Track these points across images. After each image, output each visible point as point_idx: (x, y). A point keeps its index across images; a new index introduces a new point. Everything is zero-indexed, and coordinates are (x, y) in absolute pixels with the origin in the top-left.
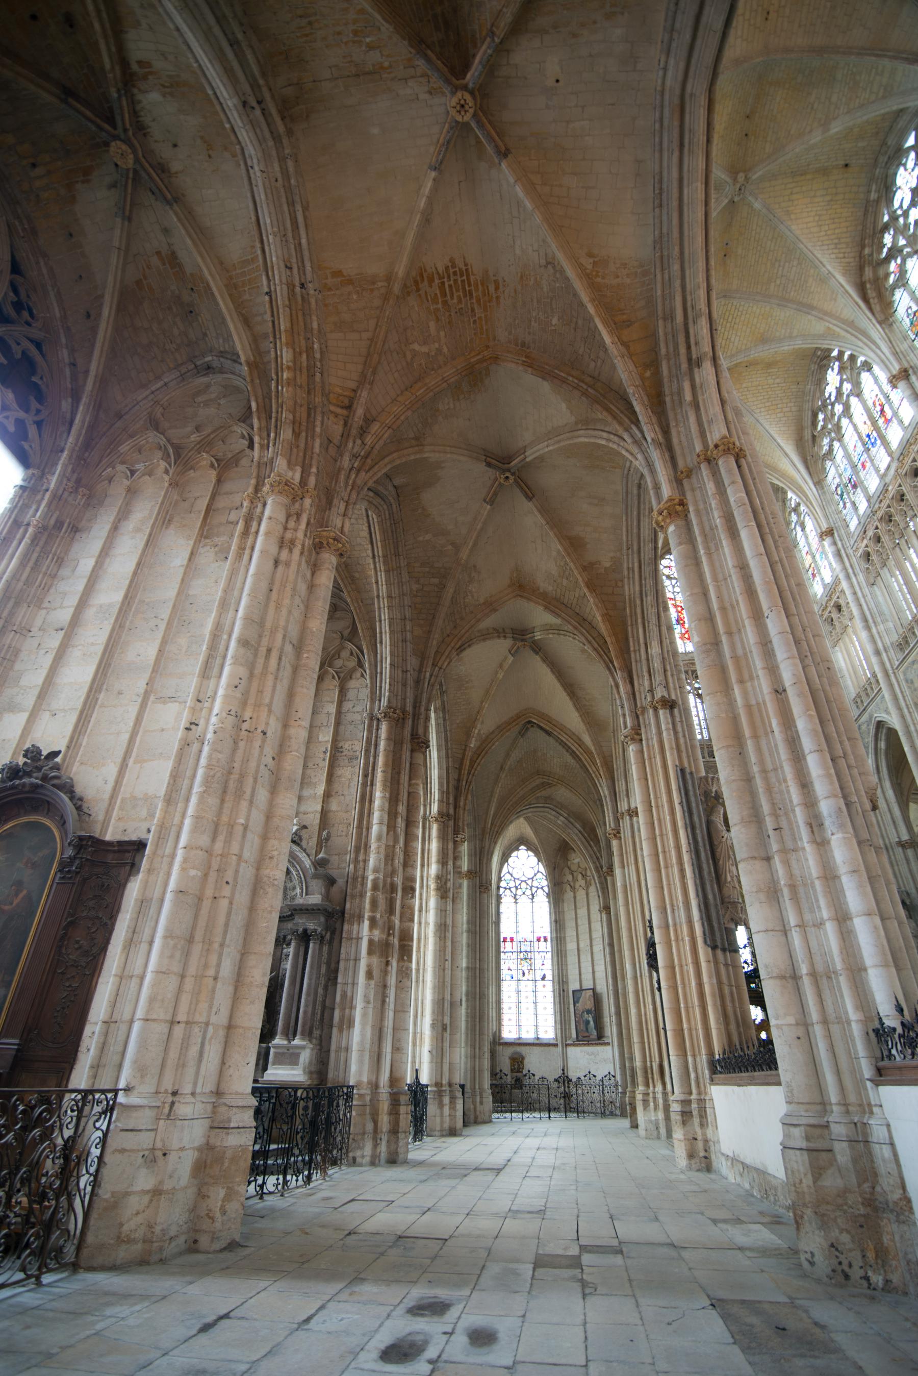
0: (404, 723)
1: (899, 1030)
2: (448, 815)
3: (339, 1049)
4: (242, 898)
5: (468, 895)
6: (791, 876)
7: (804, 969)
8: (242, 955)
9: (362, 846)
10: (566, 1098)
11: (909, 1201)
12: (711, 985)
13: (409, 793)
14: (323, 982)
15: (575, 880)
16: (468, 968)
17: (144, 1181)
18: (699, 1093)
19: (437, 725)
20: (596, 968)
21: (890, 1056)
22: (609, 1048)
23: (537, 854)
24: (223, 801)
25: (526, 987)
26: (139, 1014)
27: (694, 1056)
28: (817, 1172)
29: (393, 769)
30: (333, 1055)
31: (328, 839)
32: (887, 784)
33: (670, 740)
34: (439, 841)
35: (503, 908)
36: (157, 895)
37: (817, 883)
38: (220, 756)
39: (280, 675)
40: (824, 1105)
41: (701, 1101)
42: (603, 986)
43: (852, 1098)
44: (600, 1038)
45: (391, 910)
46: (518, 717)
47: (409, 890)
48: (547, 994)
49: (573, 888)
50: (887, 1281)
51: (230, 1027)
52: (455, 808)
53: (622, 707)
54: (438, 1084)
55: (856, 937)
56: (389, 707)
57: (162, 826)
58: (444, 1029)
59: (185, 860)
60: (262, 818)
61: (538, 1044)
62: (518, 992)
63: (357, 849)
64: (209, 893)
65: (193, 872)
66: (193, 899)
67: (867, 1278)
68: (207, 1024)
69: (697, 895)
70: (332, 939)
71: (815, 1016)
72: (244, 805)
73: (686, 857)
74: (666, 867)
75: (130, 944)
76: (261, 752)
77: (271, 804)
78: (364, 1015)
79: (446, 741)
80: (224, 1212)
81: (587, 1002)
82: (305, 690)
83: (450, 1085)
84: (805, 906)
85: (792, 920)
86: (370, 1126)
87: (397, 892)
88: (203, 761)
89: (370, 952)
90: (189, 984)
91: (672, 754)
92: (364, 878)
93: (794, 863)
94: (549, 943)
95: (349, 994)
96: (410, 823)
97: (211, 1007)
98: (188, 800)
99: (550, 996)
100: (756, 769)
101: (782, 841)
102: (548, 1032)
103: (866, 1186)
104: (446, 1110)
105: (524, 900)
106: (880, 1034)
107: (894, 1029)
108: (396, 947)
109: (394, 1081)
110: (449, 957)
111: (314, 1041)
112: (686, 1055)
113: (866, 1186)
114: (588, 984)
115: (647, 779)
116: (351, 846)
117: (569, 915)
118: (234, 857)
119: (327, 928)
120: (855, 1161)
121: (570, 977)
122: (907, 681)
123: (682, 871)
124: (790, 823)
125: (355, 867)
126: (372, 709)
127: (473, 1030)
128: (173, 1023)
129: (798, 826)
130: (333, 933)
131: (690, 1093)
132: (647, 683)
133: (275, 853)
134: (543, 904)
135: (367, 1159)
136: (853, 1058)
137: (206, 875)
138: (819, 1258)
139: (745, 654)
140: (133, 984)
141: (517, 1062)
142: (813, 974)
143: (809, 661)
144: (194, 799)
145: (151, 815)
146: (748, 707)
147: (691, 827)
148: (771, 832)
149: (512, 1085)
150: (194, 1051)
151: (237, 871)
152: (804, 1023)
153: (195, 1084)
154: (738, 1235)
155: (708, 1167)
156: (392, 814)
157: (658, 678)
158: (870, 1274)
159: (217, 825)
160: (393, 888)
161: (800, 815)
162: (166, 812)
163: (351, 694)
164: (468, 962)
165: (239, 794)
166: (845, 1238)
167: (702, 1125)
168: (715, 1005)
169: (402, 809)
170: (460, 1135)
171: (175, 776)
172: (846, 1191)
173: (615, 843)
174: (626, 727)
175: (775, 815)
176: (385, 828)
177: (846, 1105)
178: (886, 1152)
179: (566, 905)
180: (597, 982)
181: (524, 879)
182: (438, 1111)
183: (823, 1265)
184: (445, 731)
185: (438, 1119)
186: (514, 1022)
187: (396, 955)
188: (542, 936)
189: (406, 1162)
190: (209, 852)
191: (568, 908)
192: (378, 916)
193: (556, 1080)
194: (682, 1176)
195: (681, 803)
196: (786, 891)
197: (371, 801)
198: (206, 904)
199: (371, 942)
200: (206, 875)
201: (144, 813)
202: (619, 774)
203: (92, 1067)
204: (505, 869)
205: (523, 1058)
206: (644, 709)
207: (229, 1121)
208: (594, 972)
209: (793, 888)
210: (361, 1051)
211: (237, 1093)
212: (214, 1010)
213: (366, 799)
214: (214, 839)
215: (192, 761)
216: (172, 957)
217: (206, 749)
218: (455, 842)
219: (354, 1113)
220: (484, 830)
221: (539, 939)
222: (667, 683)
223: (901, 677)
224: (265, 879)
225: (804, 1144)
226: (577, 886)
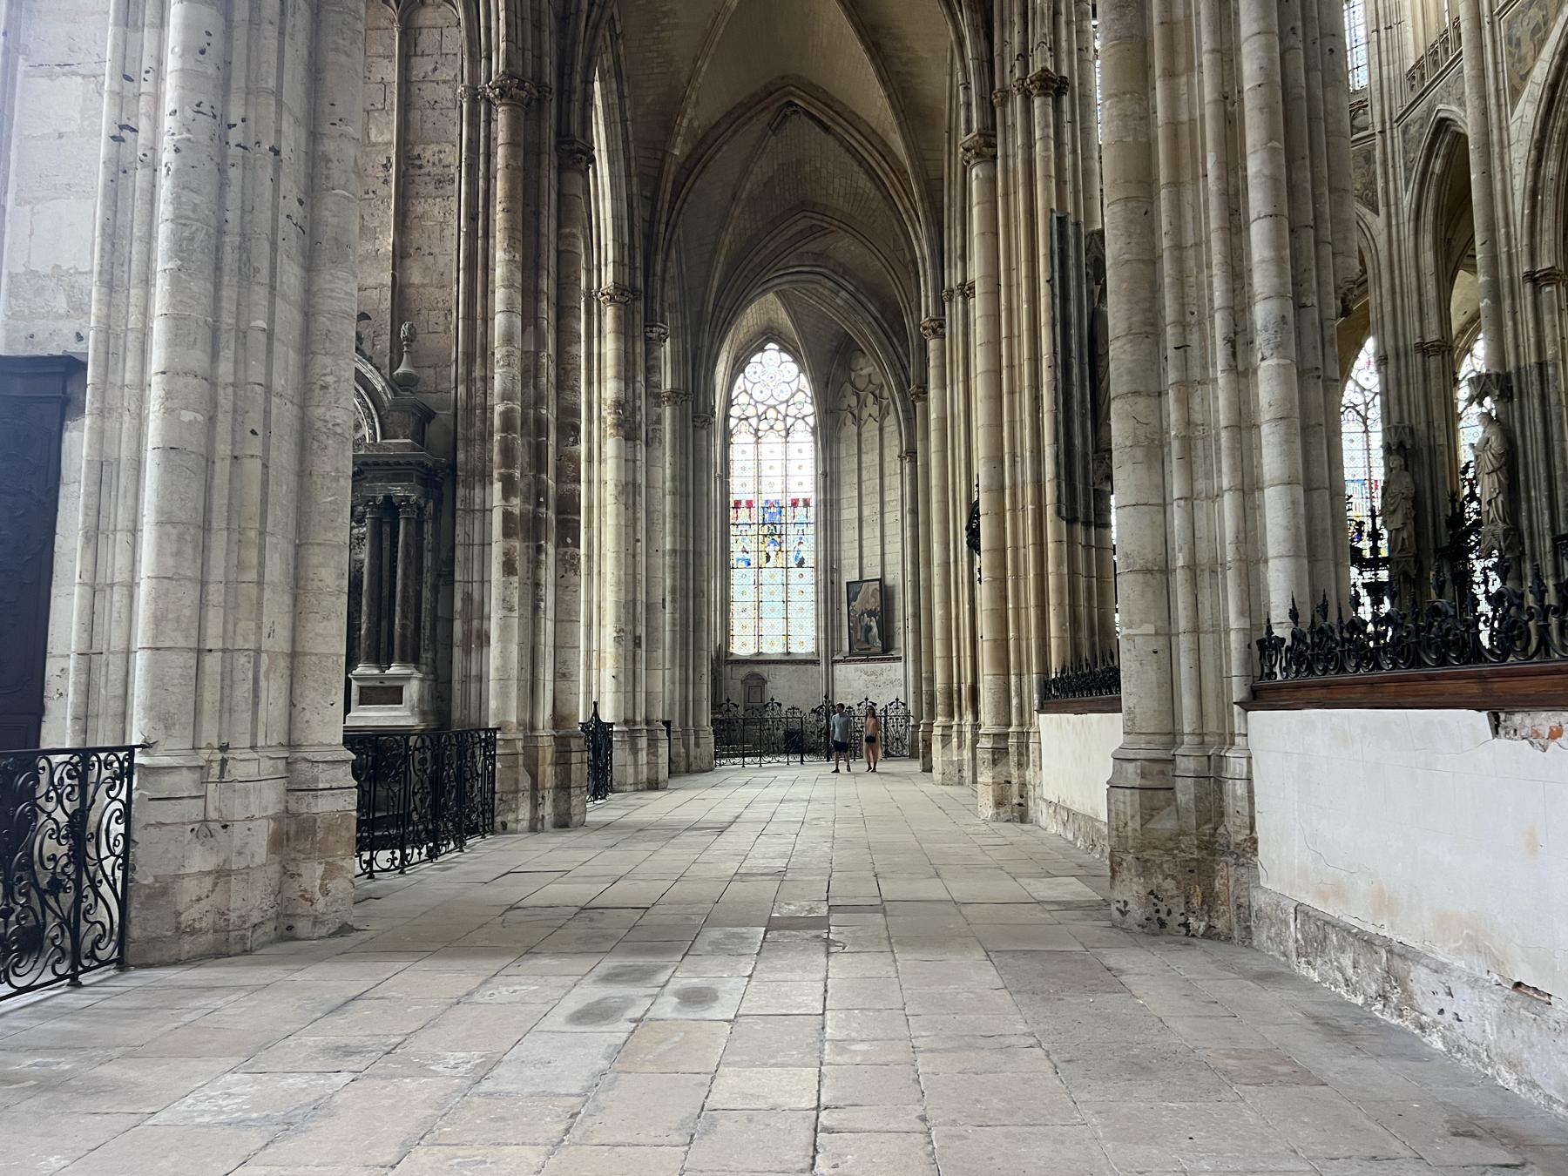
0: (540, 110)
1: (1288, 642)
2: (634, 290)
3: (466, 678)
4: (284, 456)
5: (673, 432)
6: (1188, 423)
7: (1180, 560)
8: (298, 547)
9: (477, 351)
11: (1255, 841)
12: (1059, 575)
13: (559, 253)
14: (428, 578)
15: (862, 404)
16: (674, 551)
17: (200, 860)
18: (1021, 724)
19: (607, 107)
21: (1272, 674)
23: (797, 359)
24: (217, 286)
26: (141, 638)
27: (1020, 675)
28: (1148, 813)
29: (525, 205)
30: (456, 687)
31: (411, 338)
32: (1427, 240)
33: (1046, 159)
34: (617, 339)
35: (735, 453)
36: (126, 453)
37: (1224, 435)
38: (197, 199)
39: (288, 29)
40: (1172, 736)
41: (1023, 736)
42: (894, 576)
43: (1212, 726)
44: (886, 651)
45: (539, 463)
46: (767, 92)
47: (569, 429)
48: (805, 586)
49: (858, 421)
50: (1209, 927)
51: (294, 655)
53: (967, 88)
55: (1263, 516)
56: (509, 74)
57: (108, 332)
59: (168, 395)
60: (297, 316)
61: (788, 660)
63: (469, 358)
64: (223, 449)
65: (187, 416)
66: (195, 460)
67: (1186, 925)
68: (258, 651)
69: (1056, 439)
70: (437, 510)
71: (1183, 622)
72: (260, 294)
73: (1046, 376)
74: (1012, 392)
75: (94, 535)
76: (276, 190)
77: (309, 291)
78: (505, 629)
79: (626, 141)
80: (326, 893)
81: (869, 599)
82: (343, 58)
83: (648, 722)
84: (1199, 470)
85: (1177, 488)
86: (525, 781)
87: (548, 433)
88: (164, 209)
89: (507, 533)
90: (216, 594)
91: (1047, 188)
92: (486, 409)
93: (1196, 401)
94: (812, 510)
95: (476, 596)
96: (564, 312)
97: (259, 627)
98: (147, 282)
100: (1165, 242)
101: (1185, 366)
102: (805, 641)
103: (1207, 828)
104: (643, 757)
105: (772, 441)
106: (1266, 646)
107: (1283, 640)
108: (552, 523)
109: (559, 719)
110: (642, 535)
111: (424, 668)
112: (1008, 674)
113: (1207, 828)
114: (872, 572)
115: (997, 234)
116: (457, 350)
117: (849, 464)
118: (258, 388)
119: (427, 496)
120: (1198, 799)
122: (1509, 42)
123: (1036, 399)
124: (1203, 338)
125: (468, 390)
126: (474, 77)
128: (200, 652)
129: (1214, 343)
130: (439, 502)
131: (1009, 725)
132: (1017, 39)
133: (330, 379)
134: (804, 447)
135: (525, 824)
136: (1223, 677)
137: (212, 420)
138: (1132, 906)
139: (1188, 17)
140: (116, 597)
142: (1193, 568)
143: (1297, 41)
144: (161, 285)
145: (80, 309)
146: (1174, 125)
147: (1063, 323)
148: (1170, 352)
149: (746, 720)
150: (243, 690)
151: (267, 413)
152: (1167, 633)
153: (254, 735)
154: (1042, 889)
155: (1022, 815)
156: (529, 294)
157: (1041, 30)
158: (1191, 920)
159: (215, 331)
160: (540, 427)
161: (1219, 325)
162: (109, 305)
163: (427, 41)
164: (674, 543)
165: (246, 275)
166: (1169, 884)
167: (1020, 765)
168: (1060, 604)
169: (547, 284)
170: (664, 789)
171: (113, 236)
172: (1182, 832)
173: (932, 344)
174: (969, 130)
175: (1182, 324)
176: (518, 321)
177: (1201, 735)
178: (1241, 788)
179: (843, 447)
180: (888, 569)
181: (772, 402)
183: (1137, 912)
184: (624, 121)
185: (630, 770)
187: (552, 536)
188: (801, 497)
189: (582, 824)
190: (211, 380)
191: (847, 452)
192: (518, 474)
193: (814, 711)
194: (985, 828)
195: (1050, 281)
196: (1175, 446)
197: (487, 269)
198: (222, 469)
199: (507, 517)
200: (212, 420)
201: (61, 304)
202: (952, 216)
203: (76, 718)
206: (1006, 93)
207: (316, 780)
208: (883, 554)
209: (1188, 442)
210: (503, 680)
211: (321, 744)
212: (265, 631)
213: (477, 264)
214: (214, 356)
215: (139, 206)
216: (178, 553)
217: (165, 186)
218: (648, 340)
219: (498, 765)
220: (700, 314)
221: (795, 504)
222: (1056, 41)
223: (1502, 31)
224: (319, 424)
225: (1138, 782)
226: (865, 415)
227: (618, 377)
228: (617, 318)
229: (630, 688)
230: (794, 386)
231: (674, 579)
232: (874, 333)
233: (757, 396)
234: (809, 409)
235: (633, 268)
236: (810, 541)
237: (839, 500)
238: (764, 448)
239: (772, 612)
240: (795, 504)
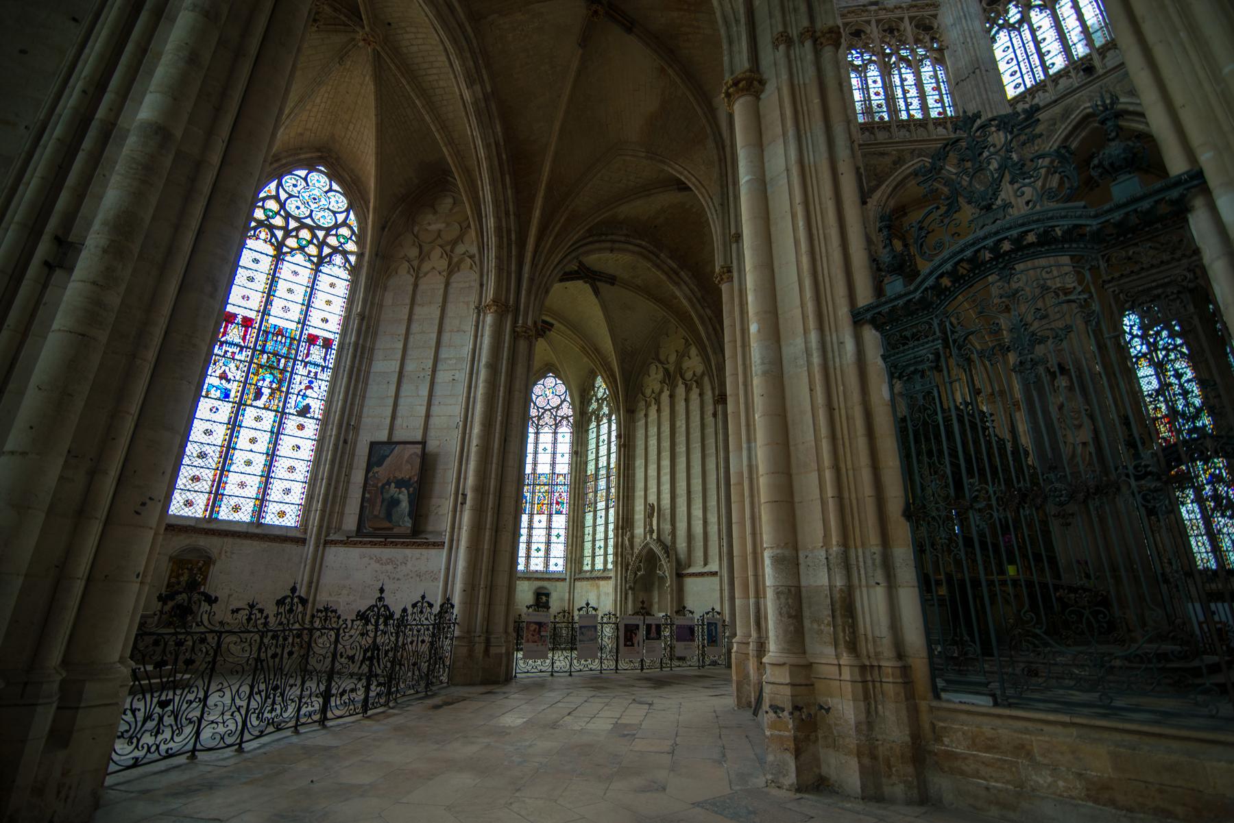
15: (423, 256)
44: (418, 533)
48: (300, 443)
62: (234, 425)
81: (404, 464)
94: (332, 356)
99: (307, 450)
102: (286, 509)
105: (296, 271)
134: (335, 287)
181: (308, 221)
186: (205, 486)
205: (209, 561)
230: (341, 218)
232: (489, 158)
233: (291, 206)
236: (321, 387)
237: (372, 350)
240: (312, 340)
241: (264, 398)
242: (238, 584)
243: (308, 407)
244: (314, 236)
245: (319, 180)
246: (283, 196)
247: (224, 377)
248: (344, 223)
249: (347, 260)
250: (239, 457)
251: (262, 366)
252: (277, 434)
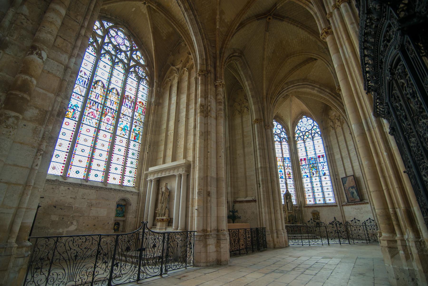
2: (208, 72)
10: (343, 232)
15: (334, 123)
16: (261, 167)
20: (354, 165)
22: (368, 205)
25: (316, 180)
34: (201, 86)
35: (298, 146)
42: (358, 173)
44: (362, 200)
48: (327, 182)
49: (334, 128)
52: (215, 68)
54: (205, 231)
58: (209, 194)
61: (326, 205)
62: (311, 182)
79: (200, 30)
81: (350, 182)
102: (330, 199)
104: (212, 248)
114: (350, 172)
121: (340, 172)
127: (268, 199)
134: (319, 142)
141: (316, 215)
164: (261, 164)
173: (328, 39)
180: (356, 171)
181: (307, 130)
182: (203, 250)
184: (198, 23)
185: (203, 255)
186: (311, 197)
193: (330, 224)
204: (297, 128)
205: (319, 213)
208: (352, 167)
218: (216, 86)
226: (336, 126)
227: (201, 97)
228: (202, 79)
229: (205, 215)
230: (313, 125)
231: (262, 176)
232: (330, 98)
233: (302, 130)
234: (318, 130)
235: (207, 65)
236: (326, 168)
237: (333, 153)
238: (307, 144)
239: (320, 190)
240: (319, 157)
241: (315, 174)
242: (326, 217)
243: (325, 173)
244: (309, 133)
245: (304, 119)
246: (299, 128)
247: (305, 173)
248: (314, 126)
249: (318, 134)
250: (315, 189)
251: (311, 168)
252: (321, 181)
